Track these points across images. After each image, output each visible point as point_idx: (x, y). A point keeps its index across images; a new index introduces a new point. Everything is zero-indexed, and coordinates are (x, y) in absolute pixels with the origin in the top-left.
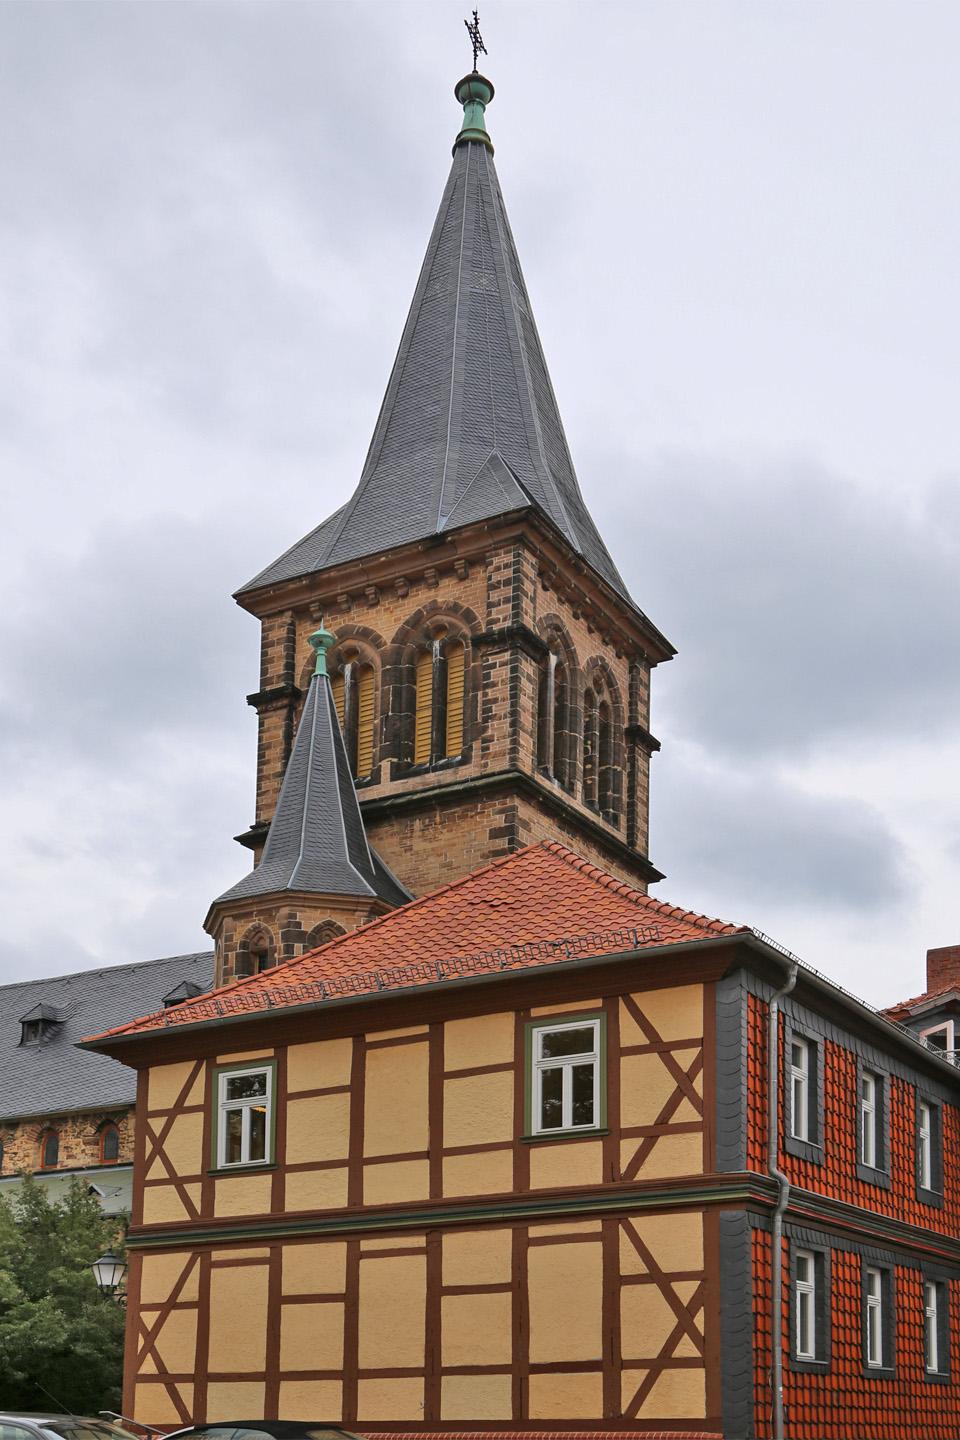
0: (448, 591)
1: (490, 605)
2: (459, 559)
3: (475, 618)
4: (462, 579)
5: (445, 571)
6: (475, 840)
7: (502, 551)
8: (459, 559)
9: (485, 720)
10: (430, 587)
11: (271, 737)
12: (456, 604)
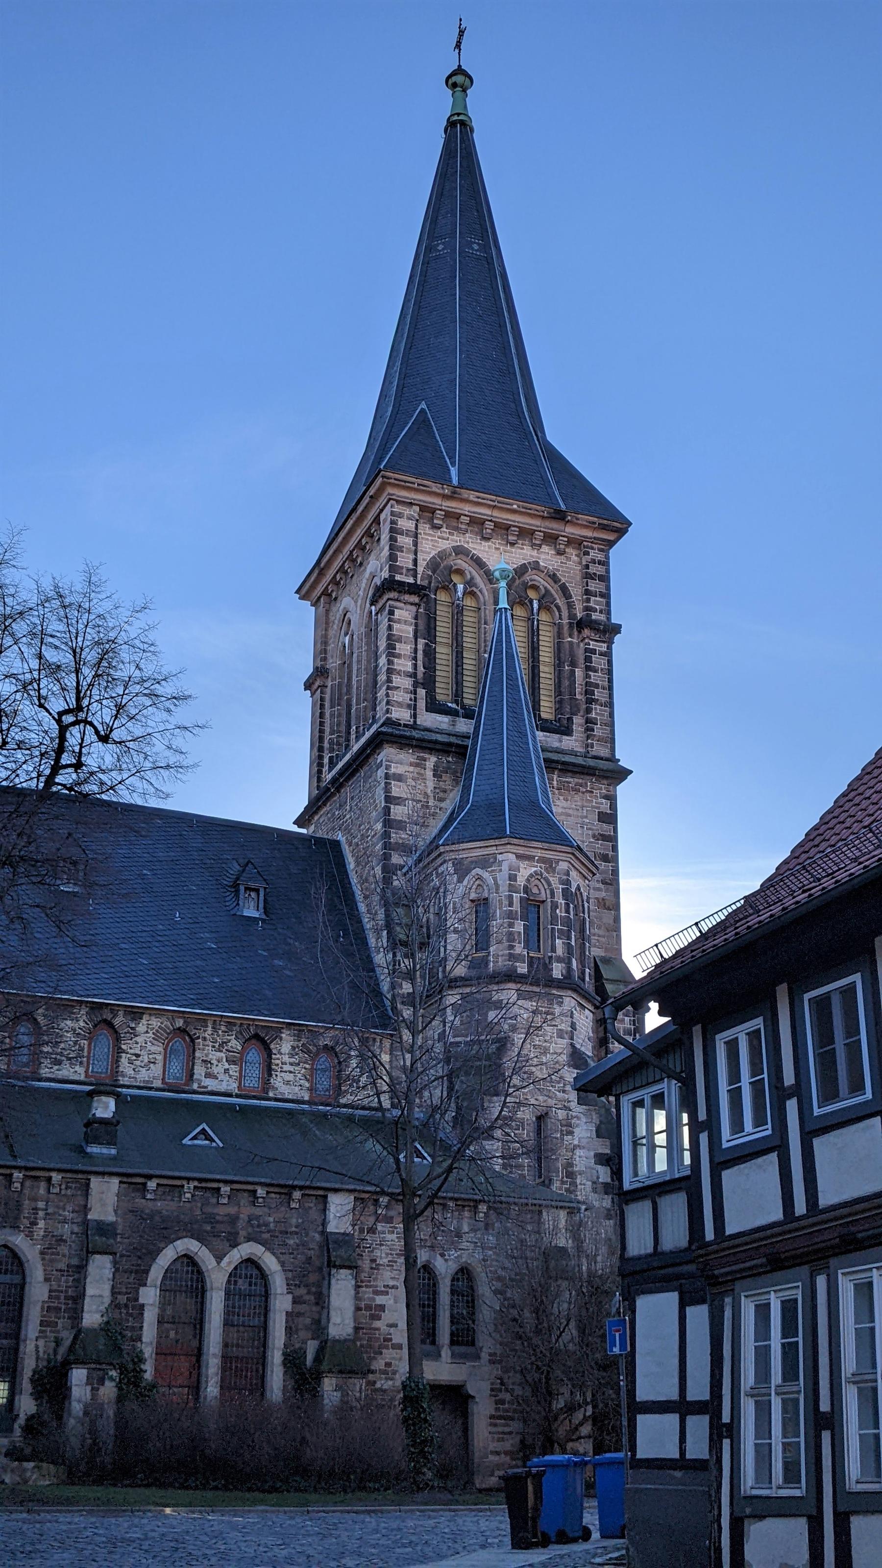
0: (547, 557)
1: (587, 592)
2: (564, 536)
3: (571, 597)
4: (560, 553)
5: (551, 539)
6: (586, 817)
7: (596, 546)
8: (564, 536)
9: (590, 701)
10: (533, 545)
11: (401, 631)
12: (554, 575)
